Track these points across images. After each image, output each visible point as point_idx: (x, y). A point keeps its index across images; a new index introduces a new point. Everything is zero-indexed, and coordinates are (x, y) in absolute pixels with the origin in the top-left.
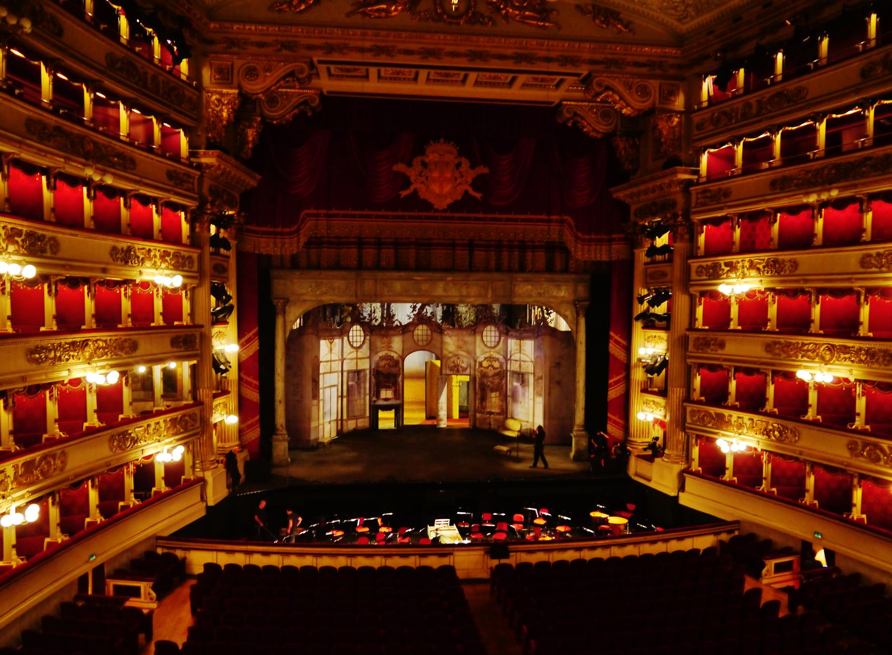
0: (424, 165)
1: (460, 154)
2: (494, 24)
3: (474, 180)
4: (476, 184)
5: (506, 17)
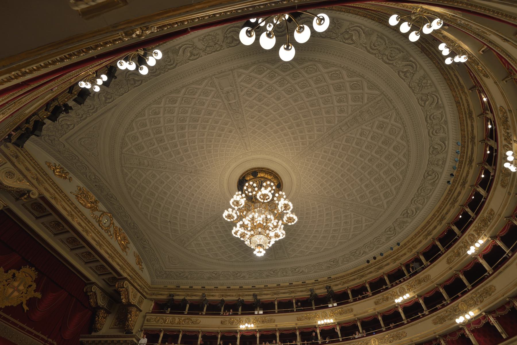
0: (14, 275)
1: (35, 281)
2: (112, 238)
3: (30, 298)
4: (31, 302)
5: (116, 238)
